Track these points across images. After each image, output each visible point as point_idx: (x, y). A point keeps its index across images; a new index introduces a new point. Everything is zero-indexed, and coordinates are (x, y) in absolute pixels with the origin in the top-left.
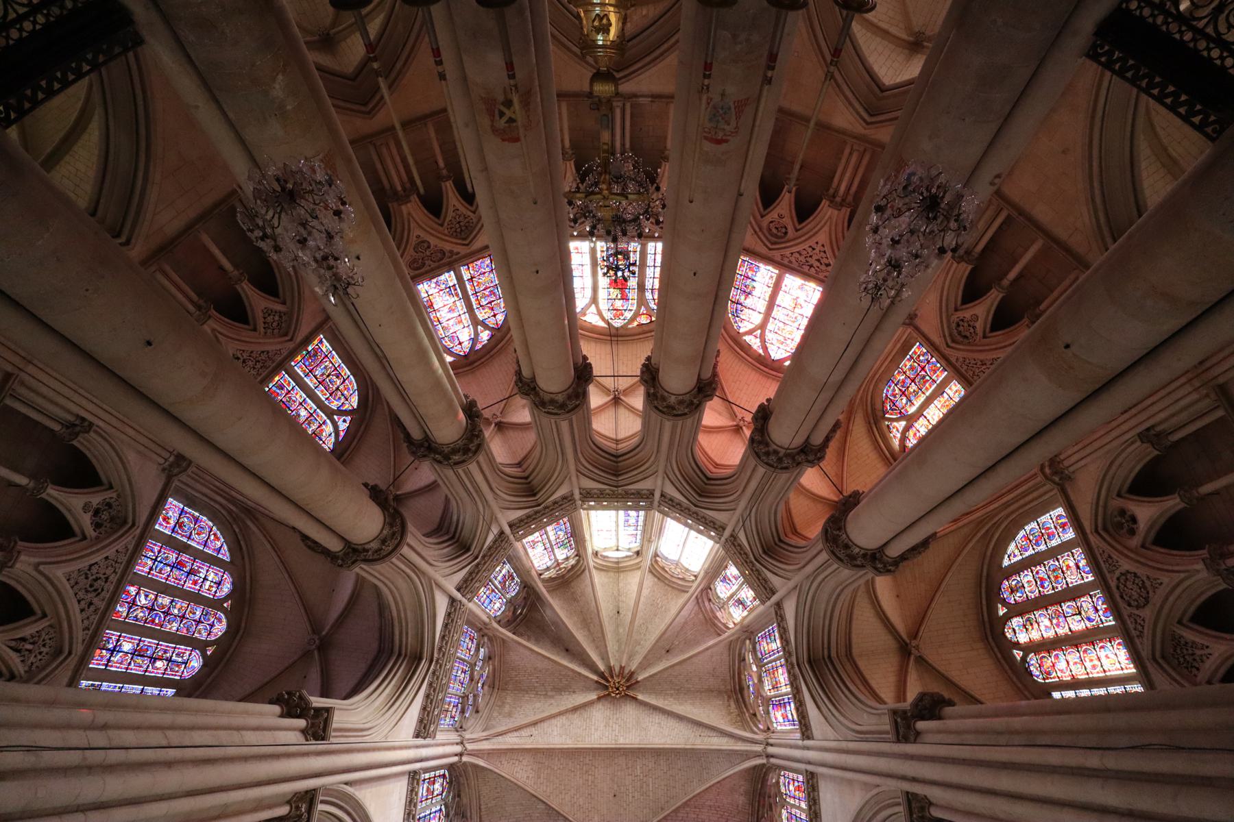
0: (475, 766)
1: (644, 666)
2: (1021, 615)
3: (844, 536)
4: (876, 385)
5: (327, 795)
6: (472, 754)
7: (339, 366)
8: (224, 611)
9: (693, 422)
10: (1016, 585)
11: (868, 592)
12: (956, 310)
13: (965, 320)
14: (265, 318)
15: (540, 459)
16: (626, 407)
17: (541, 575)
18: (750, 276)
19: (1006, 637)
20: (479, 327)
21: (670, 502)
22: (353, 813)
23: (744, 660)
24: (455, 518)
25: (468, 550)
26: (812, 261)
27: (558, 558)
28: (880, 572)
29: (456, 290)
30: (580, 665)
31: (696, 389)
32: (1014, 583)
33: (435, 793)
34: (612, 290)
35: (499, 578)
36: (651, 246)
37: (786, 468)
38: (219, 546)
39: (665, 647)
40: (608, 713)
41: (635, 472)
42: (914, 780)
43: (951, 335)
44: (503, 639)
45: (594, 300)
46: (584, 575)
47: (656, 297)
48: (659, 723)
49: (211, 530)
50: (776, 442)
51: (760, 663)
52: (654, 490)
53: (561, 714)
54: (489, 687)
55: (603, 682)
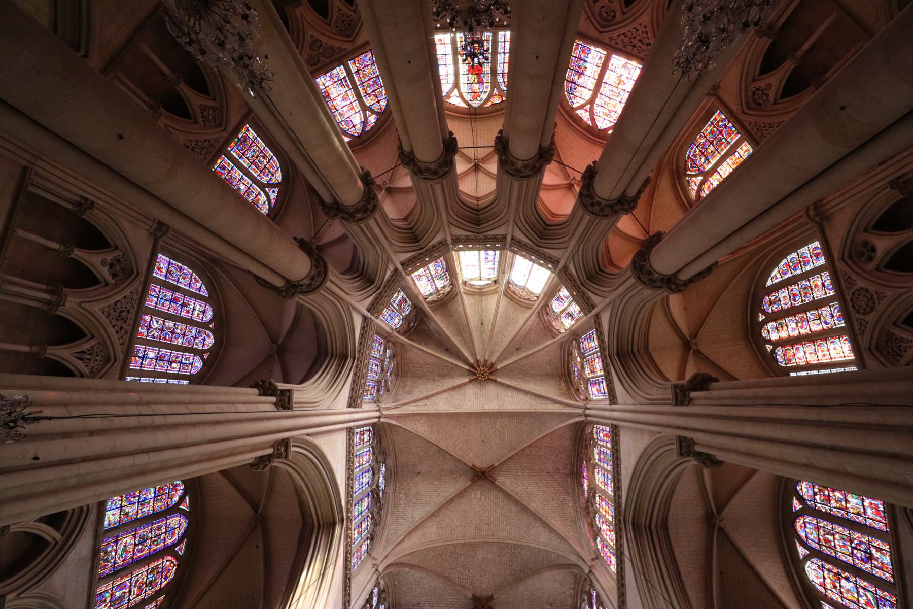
0: (390, 425)
1: (500, 359)
2: (775, 320)
3: (648, 266)
4: (681, 148)
5: (296, 442)
6: (386, 417)
7: (264, 149)
8: (211, 330)
9: (535, 182)
10: (774, 300)
11: (663, 306)
12: (754, 80)
13: (761, 88)
14: (202, 113)
15: (420, 215)
16: (484, 172)
17: (426, 299)
18: (583, 57)
19: (762, 336)
20: (367, 112)
21: (518, 244)
22: (314, 453)
23: (571, 354)
24: (362, 260)
25: (373, 283)
26: (635, 42)
27: (438, 286)
28: (673, 291)
29: (346, 81)
30: (456, 360)
31: (538, 155)
32: (773, 298)
33: (365, 441)
34: (470, 75)
35: (396, 302)
36: (501, 34)
37: (607, 215)
38: (198, 285)
39: (516, 346)
40: (477, 390)
41: (492, 222)
42: (685, 429)
43: (747, 102)
44: (402, 344)
45: (456, 85)
46: (457, 298)
47: (506, 80)
48: (512, 396)
49: (192, 276)
50: (599, 195)
51: (582, 356)
52: (506, 235)
53: (444, 391)
54: (395, 375)
55: (472, 370)
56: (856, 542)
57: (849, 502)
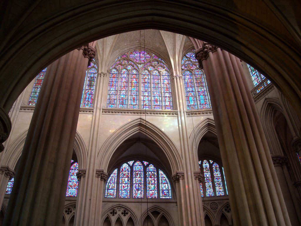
19: (204, 160)
56: (140, 185)
57: (152, 185)
